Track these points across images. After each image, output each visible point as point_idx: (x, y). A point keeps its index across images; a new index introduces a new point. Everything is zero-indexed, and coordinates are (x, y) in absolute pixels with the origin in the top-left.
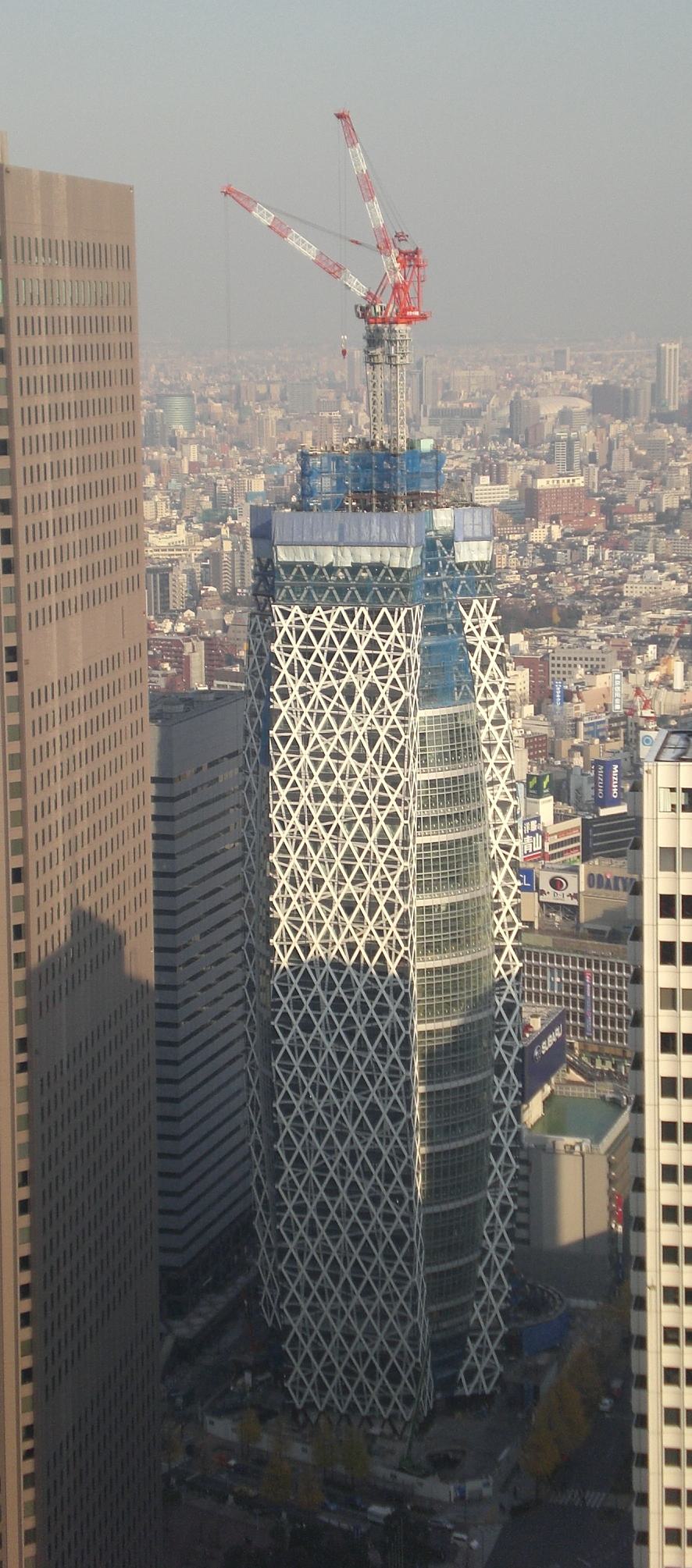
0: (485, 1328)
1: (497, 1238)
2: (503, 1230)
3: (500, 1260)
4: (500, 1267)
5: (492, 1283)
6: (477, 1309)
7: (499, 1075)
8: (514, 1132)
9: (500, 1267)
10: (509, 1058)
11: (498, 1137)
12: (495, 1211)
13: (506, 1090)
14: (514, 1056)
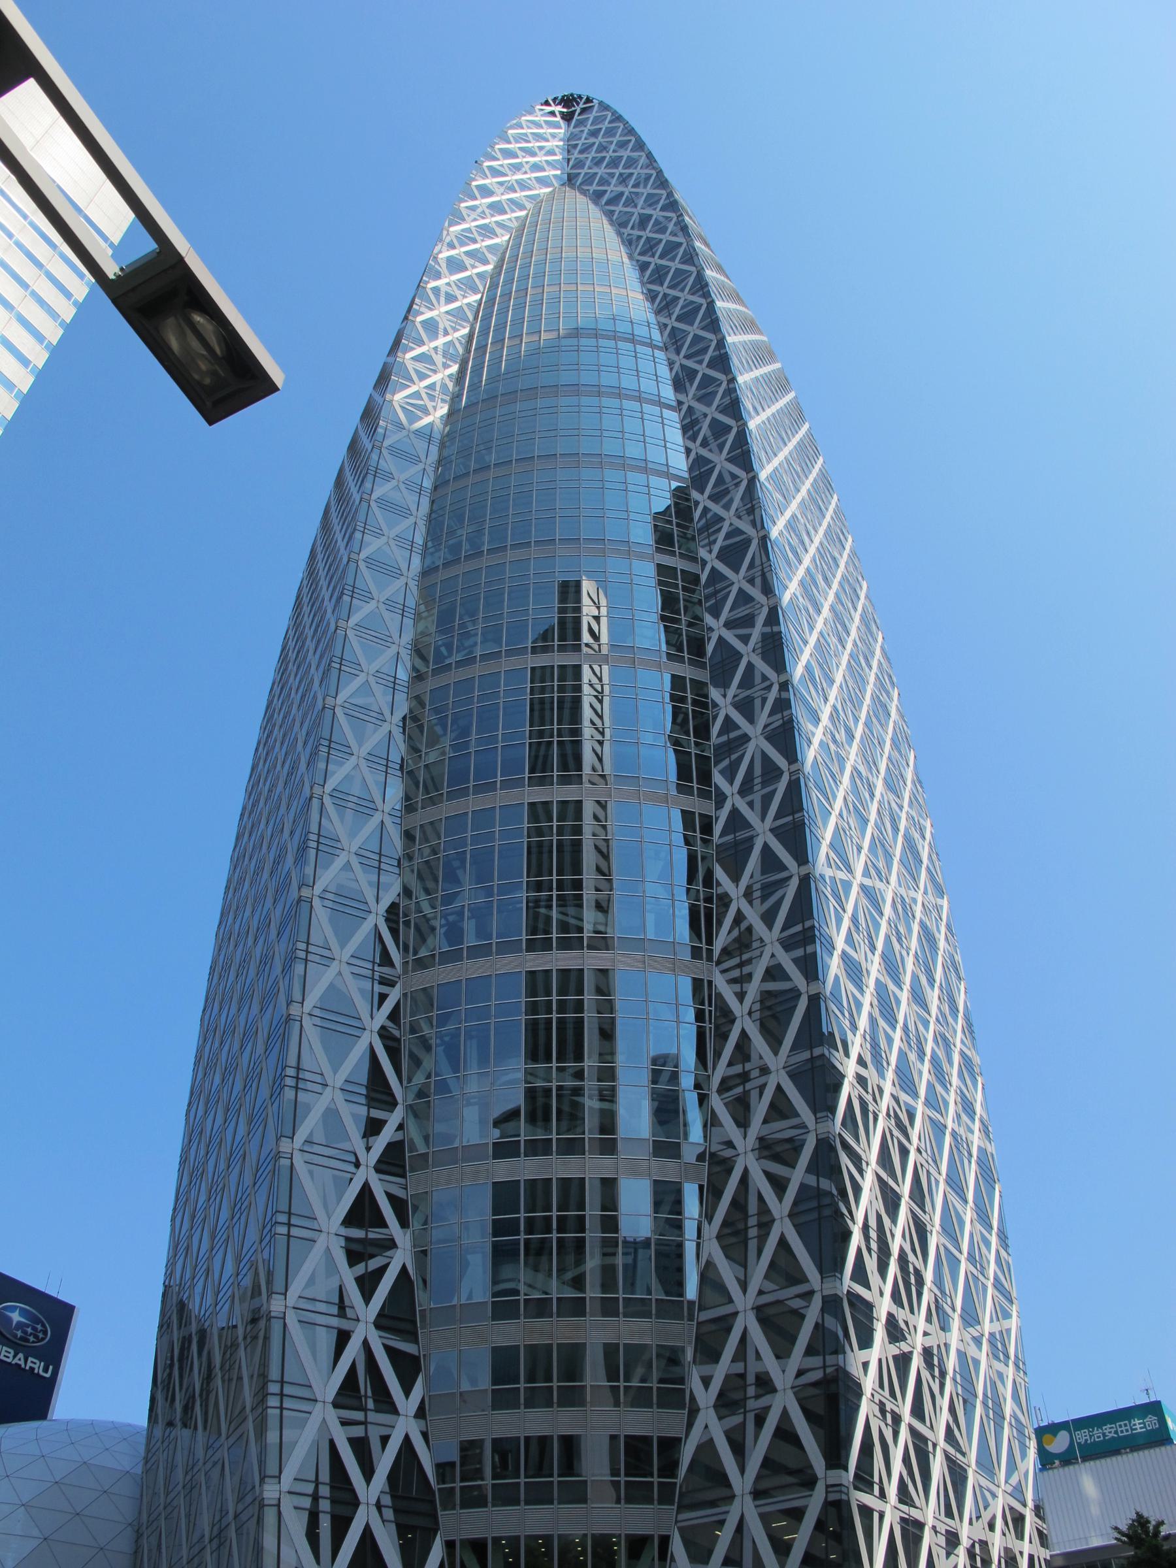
0: (741, 1483)
1: (760, 1109)
2: (779, 1077)
3: (779, 1184)
4: (780, 1208)
5: (757, 1279)
6: (706, 1398)
7: (724, 684)
8: (782, 786)
9: (780, 1208)
10: (745, 639)
11: (736, 820)
12: (745, 1022)
13: (746, 707)
14: (756, 633)
